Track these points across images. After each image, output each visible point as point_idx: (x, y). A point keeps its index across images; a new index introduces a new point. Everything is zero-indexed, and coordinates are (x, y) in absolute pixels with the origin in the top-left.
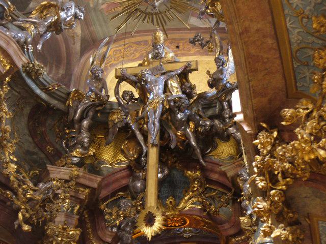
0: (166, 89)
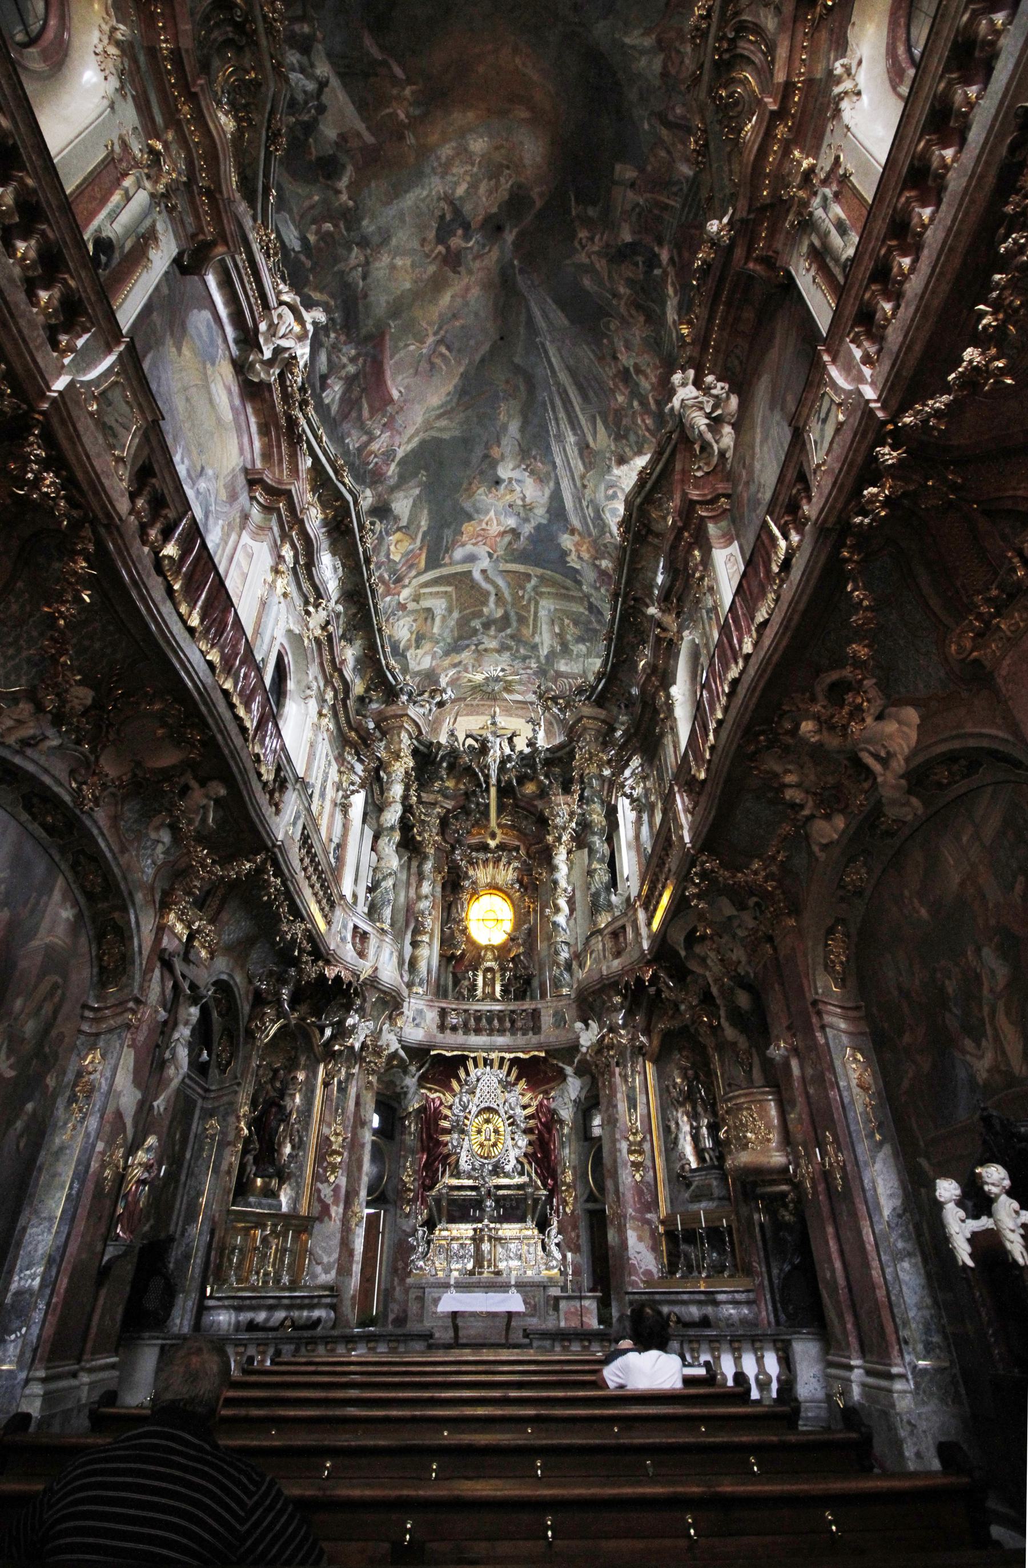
0: (501, 748)
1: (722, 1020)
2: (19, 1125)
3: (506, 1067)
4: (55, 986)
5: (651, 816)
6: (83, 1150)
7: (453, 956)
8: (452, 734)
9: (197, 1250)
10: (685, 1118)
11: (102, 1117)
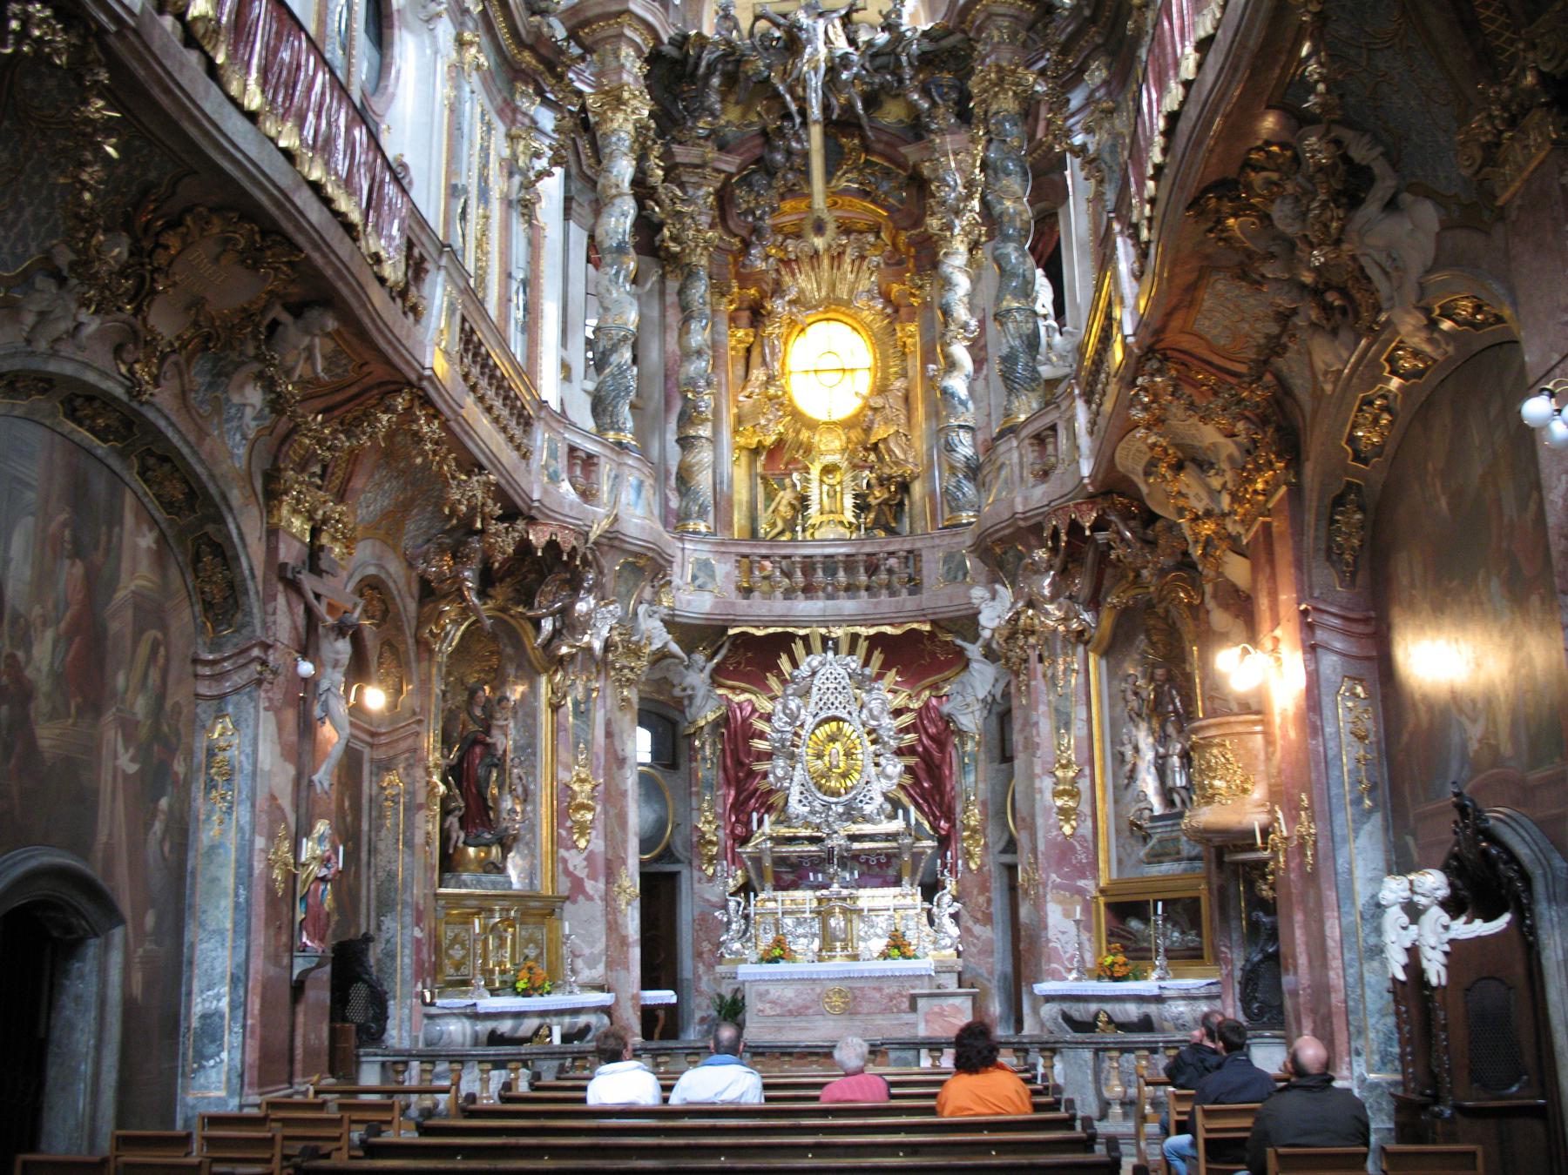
0: (828, 41)
1: (1207, 597)
2: (158, 826)
4: (155, 646)
6: (240, 849)
8: (726, 16)
9: (403, 947)
10: (1151, 740)
11: (253, 805)
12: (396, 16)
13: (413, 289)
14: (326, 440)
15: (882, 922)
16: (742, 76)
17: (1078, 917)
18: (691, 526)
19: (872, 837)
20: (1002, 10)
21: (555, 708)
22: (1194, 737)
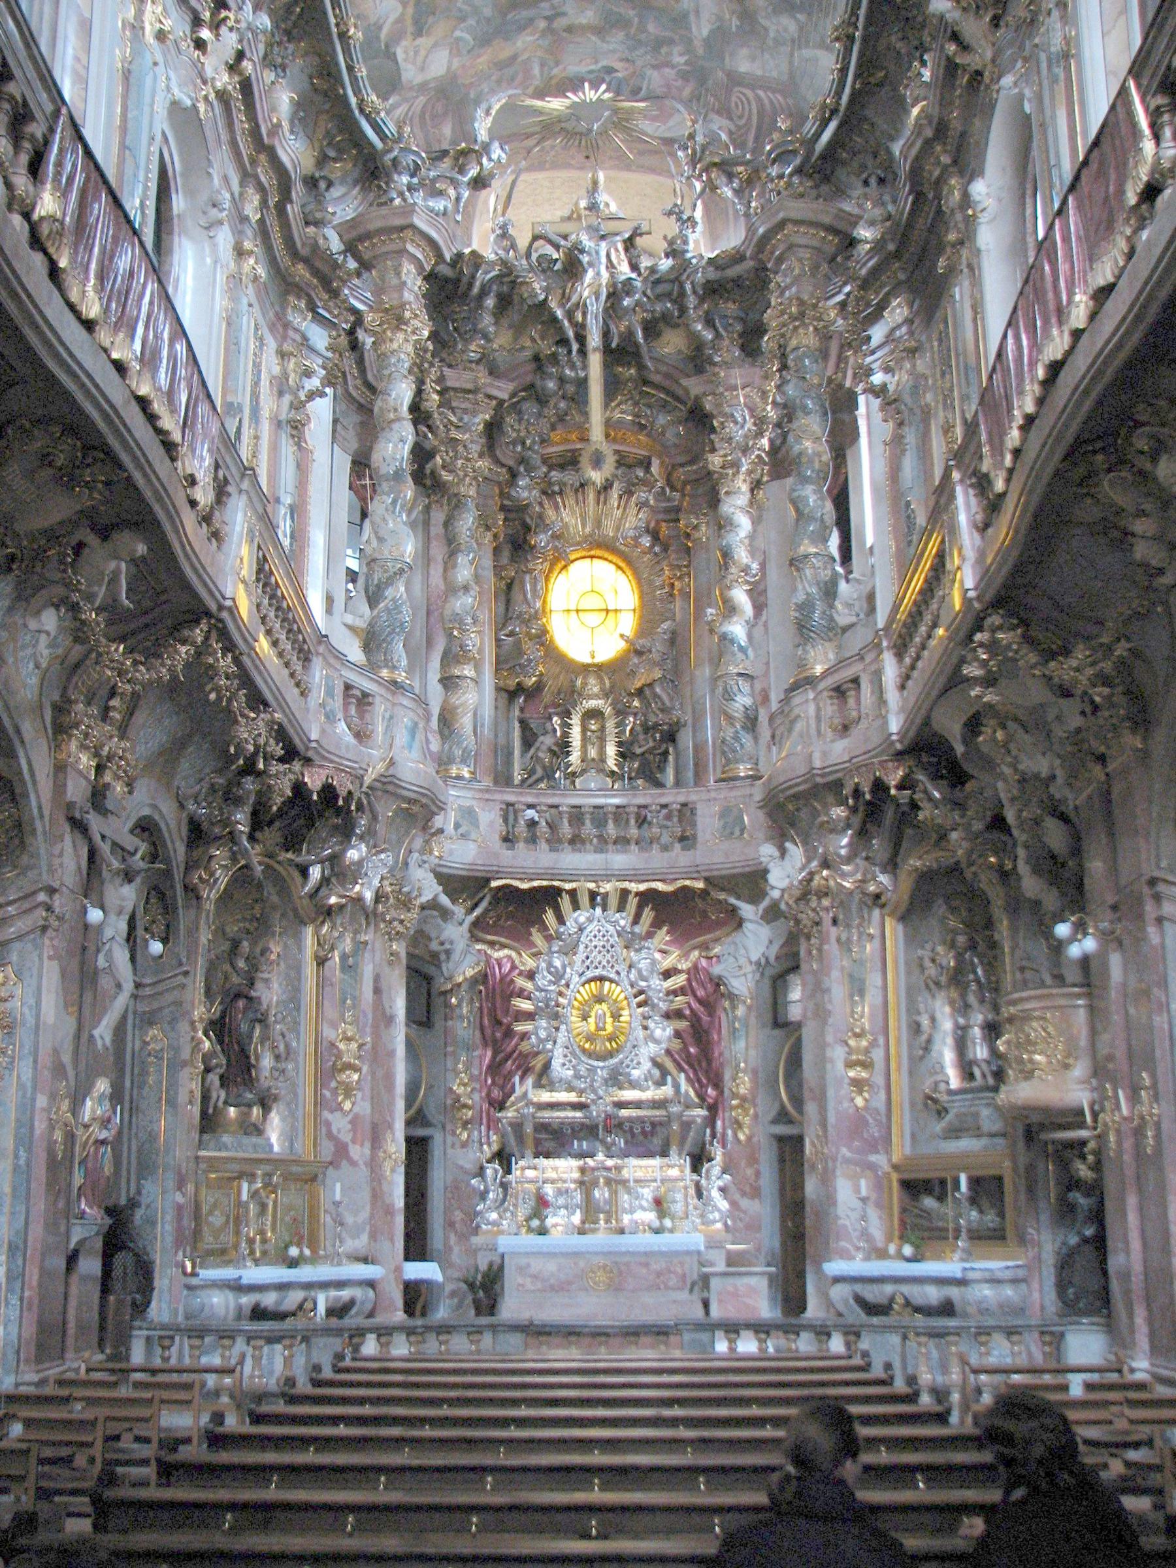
0: (611, 265)
3: (633, 902)
5: (925, 437)
7: (520, 689)
10: (947, 1009)
11: (35, 1062)
12: (176, 221)
13: (217, 513)
14: (127, 672)
15: (647, 1193)
16: (516, 298)
17: (864, 1192)
18: (454, 772)
19: (638, 1105)
20: (802, 241)
21: (321, 962)
22: (1012, 1010)
